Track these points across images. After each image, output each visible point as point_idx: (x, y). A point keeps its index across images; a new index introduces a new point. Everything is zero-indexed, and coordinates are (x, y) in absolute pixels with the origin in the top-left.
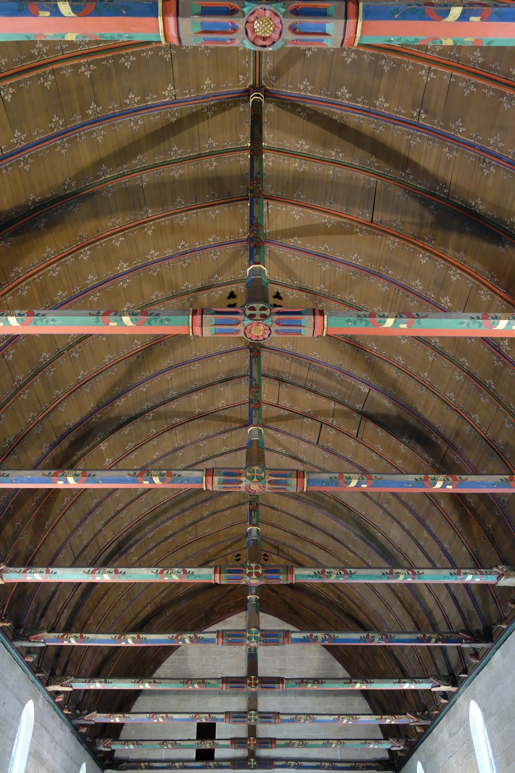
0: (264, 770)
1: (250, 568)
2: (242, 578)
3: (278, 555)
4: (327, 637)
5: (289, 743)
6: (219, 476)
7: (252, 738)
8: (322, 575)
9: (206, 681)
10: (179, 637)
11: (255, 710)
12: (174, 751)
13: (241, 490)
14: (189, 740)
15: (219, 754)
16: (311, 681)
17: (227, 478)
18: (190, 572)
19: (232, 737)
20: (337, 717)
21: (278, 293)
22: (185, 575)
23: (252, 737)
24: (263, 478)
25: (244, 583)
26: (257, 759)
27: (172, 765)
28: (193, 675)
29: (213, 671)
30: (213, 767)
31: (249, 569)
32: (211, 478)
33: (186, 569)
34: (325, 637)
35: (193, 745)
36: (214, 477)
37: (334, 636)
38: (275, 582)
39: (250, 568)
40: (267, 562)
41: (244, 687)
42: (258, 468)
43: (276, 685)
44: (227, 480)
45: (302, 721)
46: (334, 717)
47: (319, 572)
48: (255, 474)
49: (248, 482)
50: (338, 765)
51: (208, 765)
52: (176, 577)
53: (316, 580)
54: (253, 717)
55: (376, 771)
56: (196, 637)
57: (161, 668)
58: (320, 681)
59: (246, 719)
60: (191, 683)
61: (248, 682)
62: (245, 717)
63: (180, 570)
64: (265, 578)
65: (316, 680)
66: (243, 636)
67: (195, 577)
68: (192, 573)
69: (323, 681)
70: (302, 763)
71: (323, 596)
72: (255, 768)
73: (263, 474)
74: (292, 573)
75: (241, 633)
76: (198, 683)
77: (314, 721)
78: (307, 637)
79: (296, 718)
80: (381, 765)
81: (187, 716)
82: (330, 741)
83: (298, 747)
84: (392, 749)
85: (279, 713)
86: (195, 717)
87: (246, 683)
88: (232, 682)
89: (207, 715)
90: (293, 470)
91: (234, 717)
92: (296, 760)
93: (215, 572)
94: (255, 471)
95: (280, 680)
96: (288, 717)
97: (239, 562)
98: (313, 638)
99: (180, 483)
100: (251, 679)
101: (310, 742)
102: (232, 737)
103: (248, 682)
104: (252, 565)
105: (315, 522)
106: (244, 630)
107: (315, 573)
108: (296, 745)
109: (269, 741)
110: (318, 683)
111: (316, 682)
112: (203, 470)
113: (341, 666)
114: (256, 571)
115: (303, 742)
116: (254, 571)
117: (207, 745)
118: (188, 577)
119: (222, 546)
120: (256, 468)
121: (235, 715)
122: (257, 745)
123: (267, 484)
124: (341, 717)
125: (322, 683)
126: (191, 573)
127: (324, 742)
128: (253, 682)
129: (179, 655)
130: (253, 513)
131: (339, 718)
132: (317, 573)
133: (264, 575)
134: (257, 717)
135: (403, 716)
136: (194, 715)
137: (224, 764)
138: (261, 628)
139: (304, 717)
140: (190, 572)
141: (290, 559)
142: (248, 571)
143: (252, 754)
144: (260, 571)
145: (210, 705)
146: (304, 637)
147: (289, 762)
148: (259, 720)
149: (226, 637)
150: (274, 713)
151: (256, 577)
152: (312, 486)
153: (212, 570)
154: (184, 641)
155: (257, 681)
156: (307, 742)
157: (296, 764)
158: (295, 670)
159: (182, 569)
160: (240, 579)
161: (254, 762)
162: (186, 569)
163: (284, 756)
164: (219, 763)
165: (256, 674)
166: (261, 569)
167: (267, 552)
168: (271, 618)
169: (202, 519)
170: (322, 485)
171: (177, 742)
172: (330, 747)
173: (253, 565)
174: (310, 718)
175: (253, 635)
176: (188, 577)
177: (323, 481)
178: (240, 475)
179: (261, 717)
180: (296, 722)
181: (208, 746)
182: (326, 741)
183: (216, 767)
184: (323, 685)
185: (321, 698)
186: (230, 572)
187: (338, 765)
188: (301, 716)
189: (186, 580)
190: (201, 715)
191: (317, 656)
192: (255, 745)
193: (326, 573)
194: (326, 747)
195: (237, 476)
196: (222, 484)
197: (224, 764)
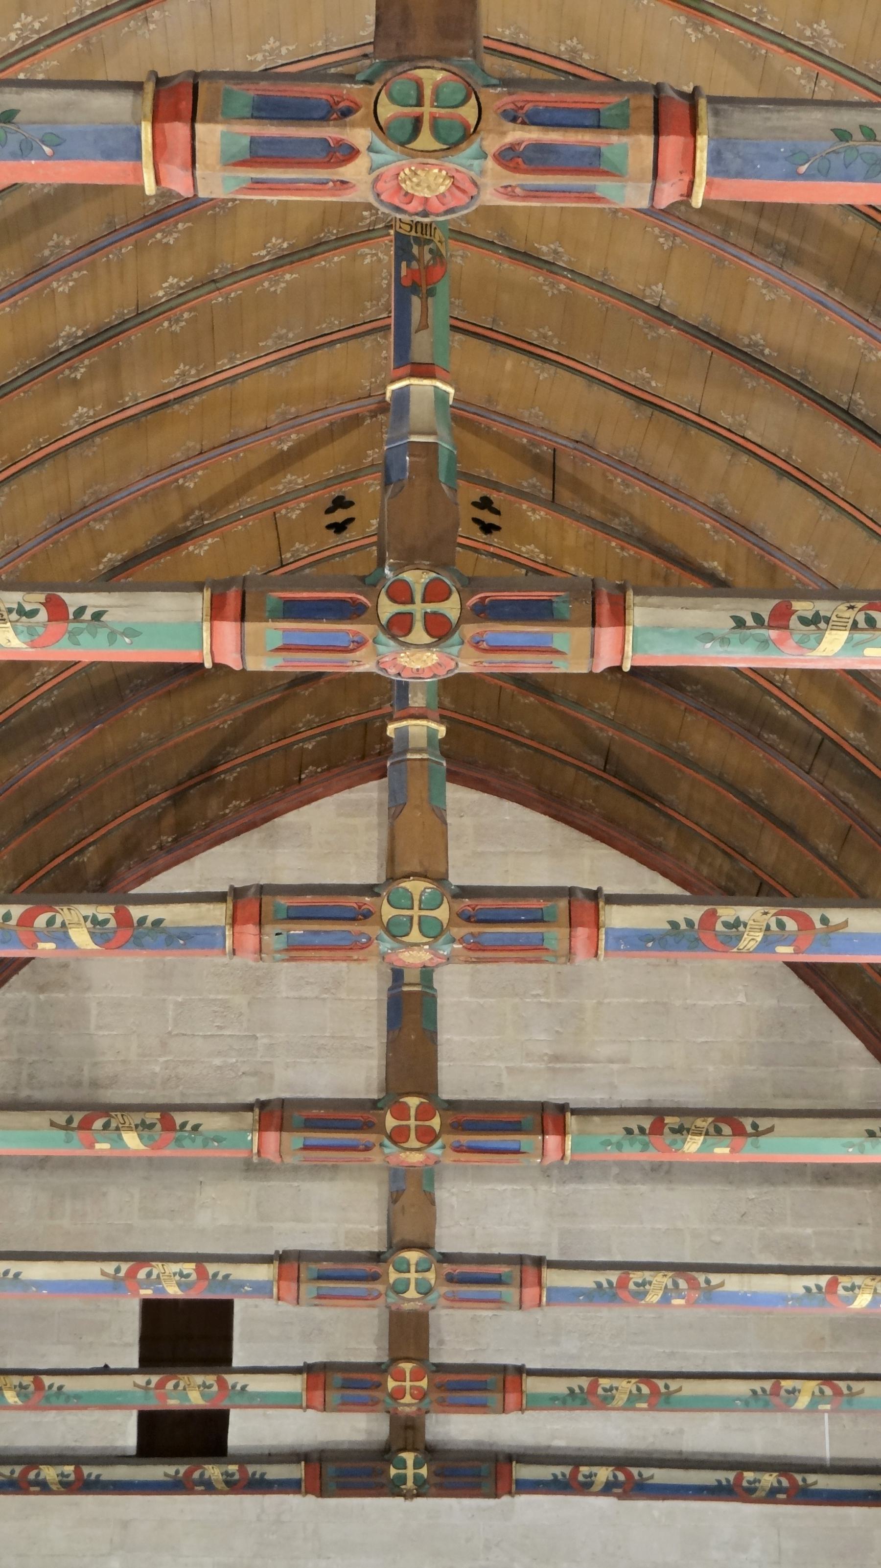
1: (401, 593)
2: (360, 644)
3: (553, 503)
4: (791, 925)
5: (589, 1388)
6: (228, 119)
7: (407, 1367)
8: (773, 634)
9: (179, 1118)
10: (41, 921)
11: (426, 1247)
12: (30, 1417)
13: (347, 197)
14: (106, 1370)
15: (244, 1431)
16: (700, 1123)
17: (273, 130)
18: (81, 610)
19: (311, 1360)
20: (823, 1280)
22: (55, 626)
23: (408, 1359)
24: (467, 134)
25: (368, 666)
26: (430, 1452)
27: (24, 1473)
28: (114, 1081)
29: (217, 1061)
30: (221, 1486)
31: (393, 599)
32: (179, 130)
33: (66, 596)
34: (781, 925)
35: (121, 1393)
36: (199, 127)
37: (824, 920)
38: (530, 665)
39: (401, 593)
40: (494, 538)
41: (367, 1149)
42: (440, 76)
43: (526, 1141)
44: (272, 142)
45: (654, 1297)
46: (811, 1281)
47: (757, 618)
48: (427, 110)
49: (388, 155)
50: (823, 1482)
51: (196, 1475)
52: (11, 634)
53: (741, 656)
54: (413, 1276)
56: (124, 920)
58: (747, 1122)
59: (380, 1287)
60: (106, 1126)
61: (391, 1122)
62: (374, 1278)
63: (34, 600)
64: (476, 645)
65: (728, 1120)
66: (366, 915)
67: (112, 636)
68: (97, 616)
69: (764, 1123)
70: (647, 1472)
71: (783, 713)
72: (422, 1490)
73: (469, 112)
74: (620, 618)
75: (351, 901)
76: (144, 1127)
77: (710, 1295)
78: (690, 923)
79: (623, 1283)
81: (91, 1271)
82: (787, 1384)
83: (630, 1405)
85: (539, 1262)
86: (132, 1274)
87: (382, 1130)
88: (311, 1125)
89: (189, 1268)
90: (637, 87)
91: (321, 1277)
92: (621, 1461)
93: (216, 612)
94: (428, 92)
95: (550, 1117)
96: (586, 1280)
97: (346, 535)
98: (719, 927)
99: (14, 156)
100: (402, 1113)
101: (690, 1388)
102: (315, 1358)
103: (391, 1122)
104: (408, 576)
105: (758, 337)
106: (370, 890)
107: (740, 623)
108: (621, 1399)
109: (489, 1377)
110: (739, 1131)
111: (726, 1129)
112: (136, 87)
114: (430, 607)
115: (655, 1386)
116: (419, 608)
117: (191, 1392)
118: (73, 635)
119: (257, 453)
120: (431, 77)
121: (326, 1266)
122: (435, 1395)
123: (490, 163)
124: (845, 1281)
125: (758, 1132)
126: (87, 616)
127: (757, 1385)
128: (412, 1123)
129: (42, 989)
130: (416, 301)
131: (832, 1285)
132: (750, 622)
133: (470, 630)
134: (431, 1276)
136: (125, 1267)
137: (274, 1472)
138: (456, 879)
139: (661, 1280)
140: (81, 610)
141: (615, 523)
142: (387, 609)
143: (407, 1432)
144: (451, 608)
145: (203, 1219)
146: (674, 925)
147: (584, 1470)
148: (445, 1289)
149: (276, 921)
150: (519, 1260)
151: (427, 639)
152: (740, 174)
153: (199, 602)
154: (63, 939)
155: (436, 1123)
156: (674, 1385)
157: (621, 1477)
158: (626, 1061)
159: (41, 597)
160: (345, 650)
161: (417, 1465)
162: (66, 596)
163: (559, 1443)
164: (251, 1469)
165: (426, 1085)
166: (455, 597)
167: (496, 486)
168: (510, 813)
169: (144, 314)
170: (795, 176)
171: (47, 1380)
172: (786, 1407)
173: (417, 579)
174: (693, 1285)
175: (416, 913)
176: (73, 635)
177: (796, 156)
178: (346, 113)
179: (451, 1279)
180: (623, 1302)
181: (196, 1399)
182: (768, 1384)
183: (233, 1486)
184: (762, 1139)
186: (294, 610)
187: (823, 1482)
188: (647, 1275)
189: (63, 650)
190: (157, 1268)
191: (741, 998)
192: (421, 1395)
193: (794, 622)
194: (766, 1407)
195: (324, 119)
196: (243, 163)
197: (274, 1472)
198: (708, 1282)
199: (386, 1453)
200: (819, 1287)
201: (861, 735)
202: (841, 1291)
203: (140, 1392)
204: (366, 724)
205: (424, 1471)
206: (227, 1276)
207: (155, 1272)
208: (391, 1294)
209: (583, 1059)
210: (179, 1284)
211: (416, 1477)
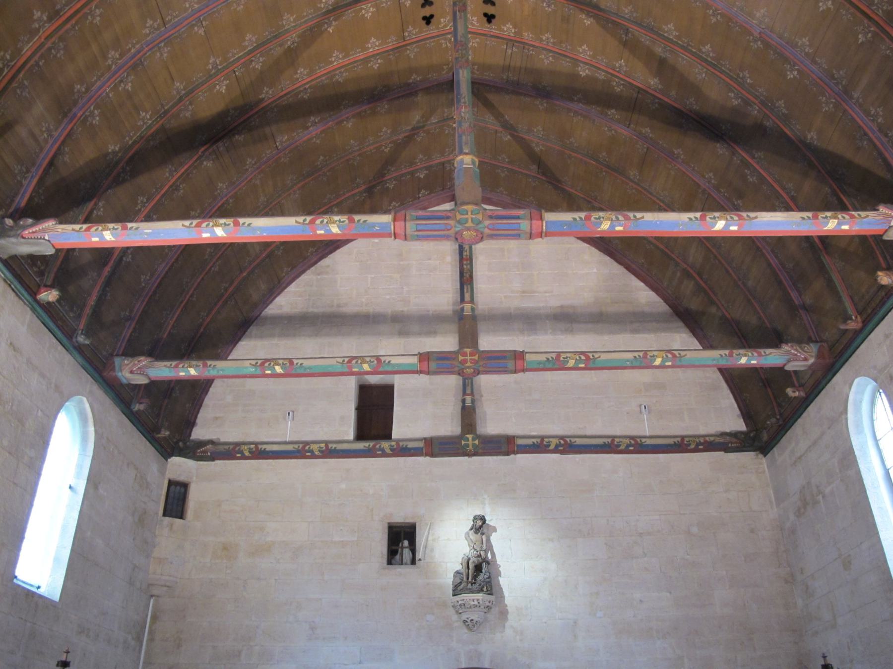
0: (495, 458)
7: (468, 350)
21: (489, 21)
29: (388, 297)
30: (388, 451)
51: (378, 446)
55: (722, 453)
57: (283, 294)
80: (734, 440)
84: (787, 368)
91: (418, 218)
113: (642, 284)
127: (636, 354)
135: (870, 213)
156: (596, 356)
157: (562, 442)
158: (552, 292)
161: (473, 439)
185: (606, 337)
191: (595, 270)
192: (475, 362)
198: (635, 216)
199: (461, 437)
200: (696, 218)
201: (656, 80)
202: (708, 219)
203: (339, 366)
204: (443, 164)
205: (476, 442)
206: (365, 221)
207: (325, 220)
208: (458, 225)
209: (534, 292)
210: (339, 227)
211: (473, 445)
